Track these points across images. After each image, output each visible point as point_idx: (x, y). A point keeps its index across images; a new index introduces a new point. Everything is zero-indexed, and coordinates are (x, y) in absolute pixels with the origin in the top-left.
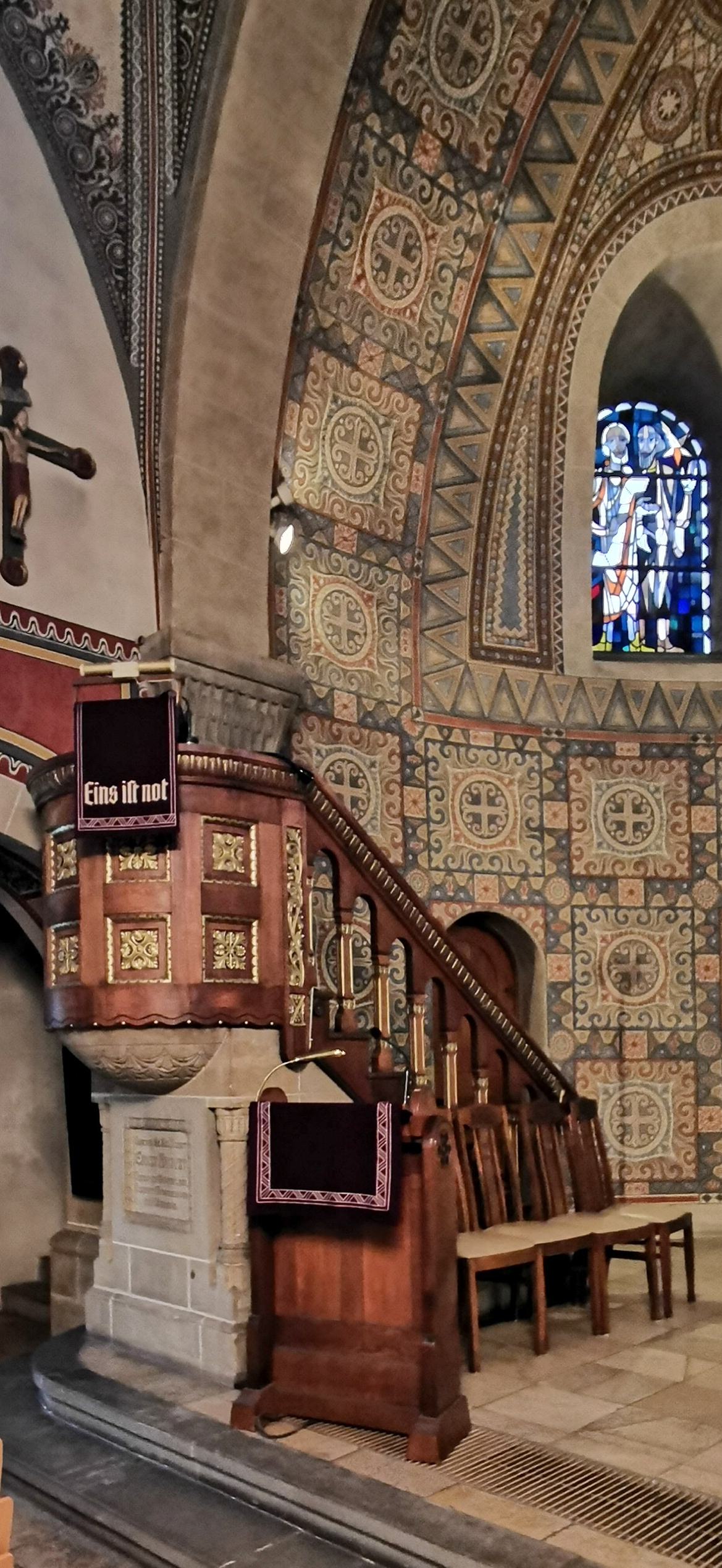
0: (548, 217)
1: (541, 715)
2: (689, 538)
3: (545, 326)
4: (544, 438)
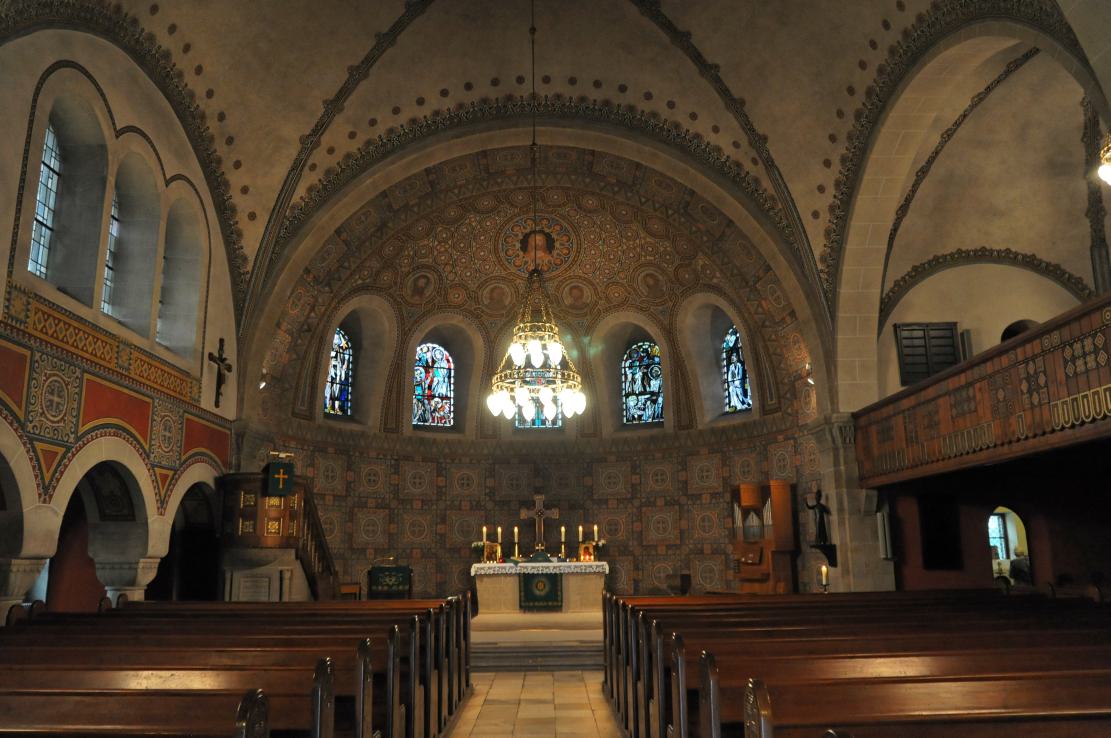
0: (332, 292)
1: (309, 436)
2: (347, 374)
3: (325, 318)
4: (319, 349)
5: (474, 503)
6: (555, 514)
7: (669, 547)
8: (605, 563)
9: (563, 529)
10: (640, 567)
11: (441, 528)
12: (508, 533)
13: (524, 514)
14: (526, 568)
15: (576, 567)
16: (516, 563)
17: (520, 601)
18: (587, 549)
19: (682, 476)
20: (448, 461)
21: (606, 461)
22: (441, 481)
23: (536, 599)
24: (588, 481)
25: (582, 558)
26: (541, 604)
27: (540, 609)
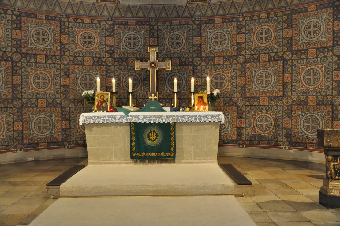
5: (96, 59)
6: (167, 65)
7: (271, 98)
8: (221, 113)
9: (176, 81)
10: (243, 115)
11: (65, 81)
12: (122, 85)
13: (138, 65)
14: (138, 117)
15: (190, 116)
16: (127, 112)
17: (131, 151)
18: (201, 97)
19: (288, 33)
20: (71, 20)
21: (214, 23)
22: (64, 38)
23: (147, 149)
24: (197, 41)
25: (196, 107)
26: (153, 154)
27: (152, 160)
